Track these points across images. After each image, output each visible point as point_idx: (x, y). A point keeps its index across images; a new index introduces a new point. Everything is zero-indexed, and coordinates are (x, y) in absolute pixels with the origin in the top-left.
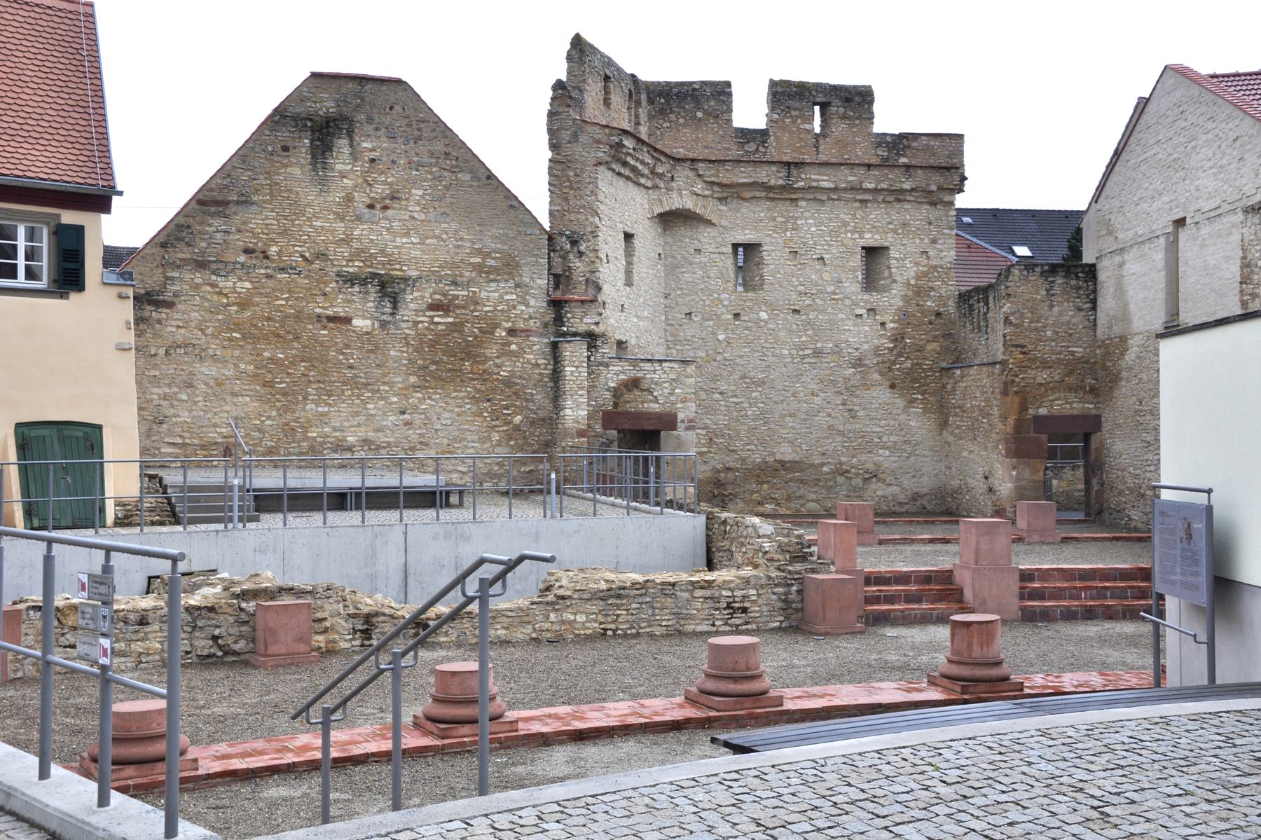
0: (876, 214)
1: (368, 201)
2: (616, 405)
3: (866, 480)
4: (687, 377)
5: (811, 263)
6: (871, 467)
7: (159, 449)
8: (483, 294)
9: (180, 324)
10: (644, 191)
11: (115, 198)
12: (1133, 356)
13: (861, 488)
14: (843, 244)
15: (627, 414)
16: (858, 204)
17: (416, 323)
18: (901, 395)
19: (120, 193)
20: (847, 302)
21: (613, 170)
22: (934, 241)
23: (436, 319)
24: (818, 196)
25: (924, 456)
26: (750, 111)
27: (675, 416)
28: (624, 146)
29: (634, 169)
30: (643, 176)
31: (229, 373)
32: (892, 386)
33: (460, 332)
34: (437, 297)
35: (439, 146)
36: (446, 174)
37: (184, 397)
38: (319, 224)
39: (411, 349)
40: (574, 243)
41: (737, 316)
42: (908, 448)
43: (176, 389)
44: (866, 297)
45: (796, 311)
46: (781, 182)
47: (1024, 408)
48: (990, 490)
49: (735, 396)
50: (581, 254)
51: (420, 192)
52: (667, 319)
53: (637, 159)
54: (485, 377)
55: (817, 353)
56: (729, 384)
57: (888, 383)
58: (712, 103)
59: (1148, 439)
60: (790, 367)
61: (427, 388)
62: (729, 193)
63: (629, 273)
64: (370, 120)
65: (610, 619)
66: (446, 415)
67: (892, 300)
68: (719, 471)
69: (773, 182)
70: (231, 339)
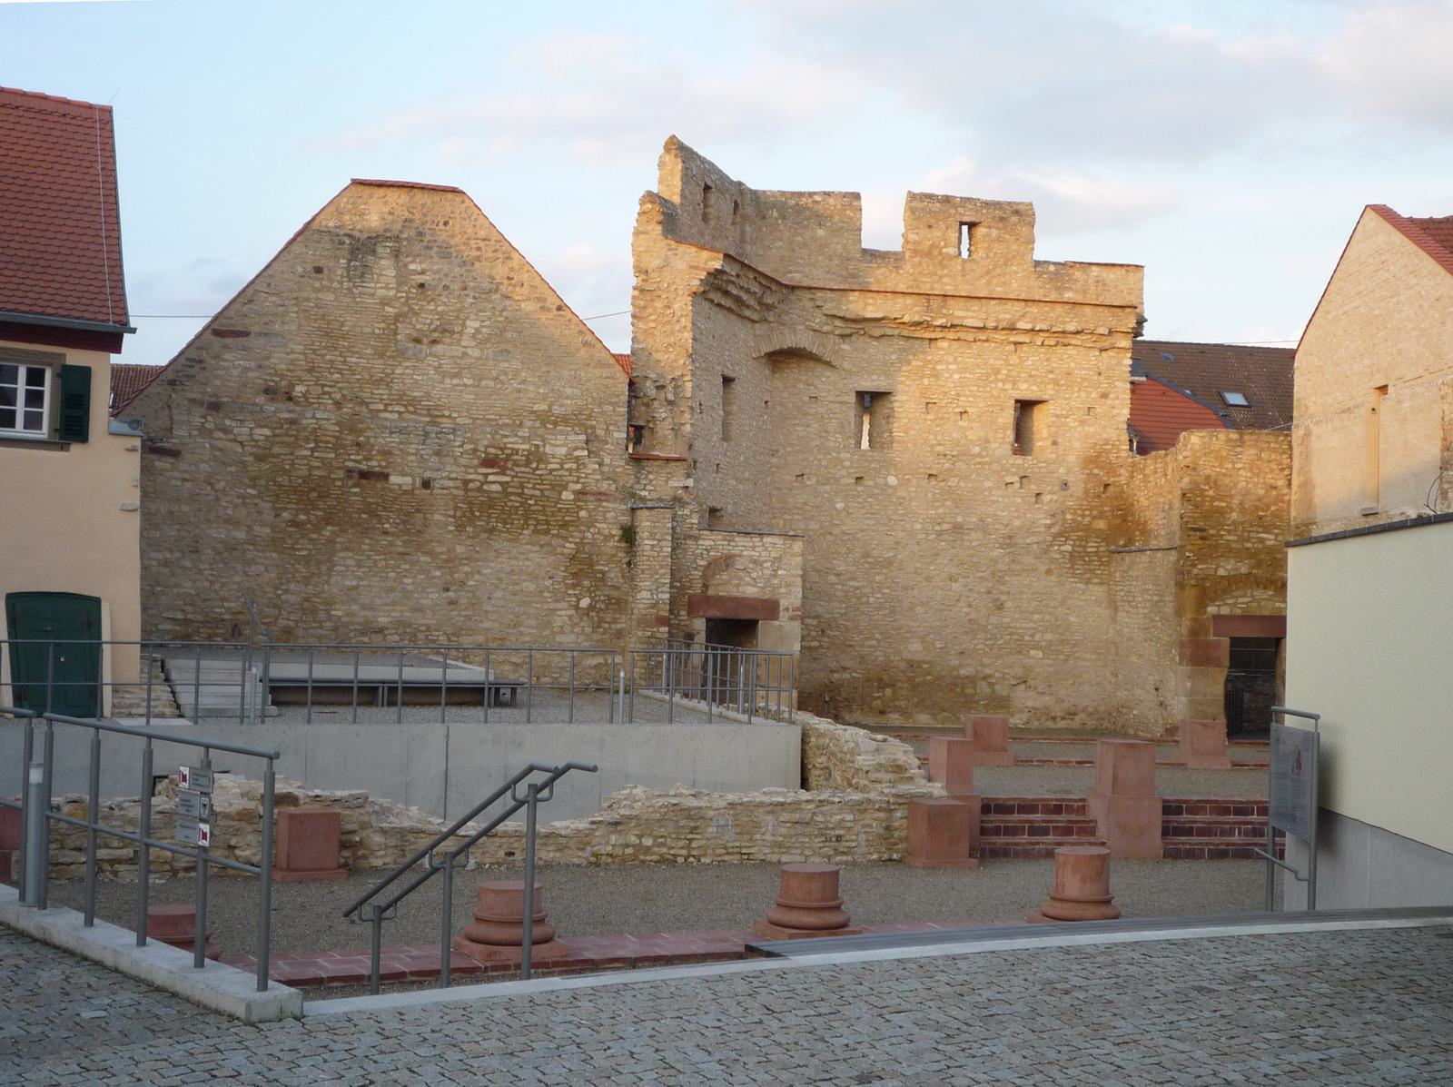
0: (1033, 358)
1: (415, 335)
2: (706, 586)
6: (1019, 672)
7: (156, 625)
8: (548, 449)
9: (187, 476)
10: (749, 325)
11: (126, 336)
14: (992, 396)
17: (466, 482)
19: (133, 331)
21: (712, 301)
22: (1104, 396)
23: (491, 478)
24: (962, 335)
25: (1085, 659)
29: (738, 300)
30: (748, 307)
31: (240, 535)
37: (187, 564)
38: (354, 360)
39: (459, 513)
43: (178, 555)
44: (1019, 460)
47: (1201, 605)
49: (853, 579)
55: (957, 528)
63: (726, 426)
65: (681, 843)
68: (832, 671)
70: (243, 497)
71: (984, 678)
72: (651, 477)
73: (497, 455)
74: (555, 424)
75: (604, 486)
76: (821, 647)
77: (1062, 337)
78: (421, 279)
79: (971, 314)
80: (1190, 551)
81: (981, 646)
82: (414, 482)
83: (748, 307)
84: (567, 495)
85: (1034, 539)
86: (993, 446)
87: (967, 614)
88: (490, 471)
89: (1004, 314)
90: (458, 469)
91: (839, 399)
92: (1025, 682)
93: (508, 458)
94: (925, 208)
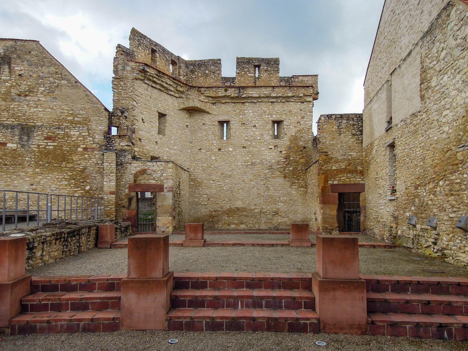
0: (278, 107)
1: (18, 92)
2: (135, 181)
4: (168, 168)
5: (250, 127)
6: (274, 210)
10: (175, 98)
13: (271, 219)
14: (264, 120)
16: (270, 104)
17: (39, 146)
18: (288, 181)
20: (266, 143)
23: (49, 144)
24: (253, 101)
26: (229, 70)
27: (163, 186)
29: (163, 86)
32: (285, 177)
34: (50, 134)
35: (52, 69)
36: (56, 81)
40: (122, 113)
41: (220, 149)
42: (292, 202)
44: (274, 141)
46: (236, 95)
47: (326, 181)
49: (219, 182)
50: (126, 117)
51: (43, 89)
53: (162, 81)
54: (72, 169)
55: (253, 164)
56: (216, 177)
58: (212, 67)
61: (44, 174)
62: (216, 100)
64: (19, 57)
66: (54, 186)
67: (285, 142)
69: (233, 95)
71: (263, 213)
72: (113, 142)
75: (94, 146)
76: (208, 204)
77: (287, 99)
78: (20, 73)
80: (321, 161)
82: (17, 146)
83: (171, 91)
84: (80, 149)
85: (280, 166)
86: (265, 136)
88: (49, 141)
89: (266, 92)
90: (36, 141)
93: (56, 136)
94: (242, 63)
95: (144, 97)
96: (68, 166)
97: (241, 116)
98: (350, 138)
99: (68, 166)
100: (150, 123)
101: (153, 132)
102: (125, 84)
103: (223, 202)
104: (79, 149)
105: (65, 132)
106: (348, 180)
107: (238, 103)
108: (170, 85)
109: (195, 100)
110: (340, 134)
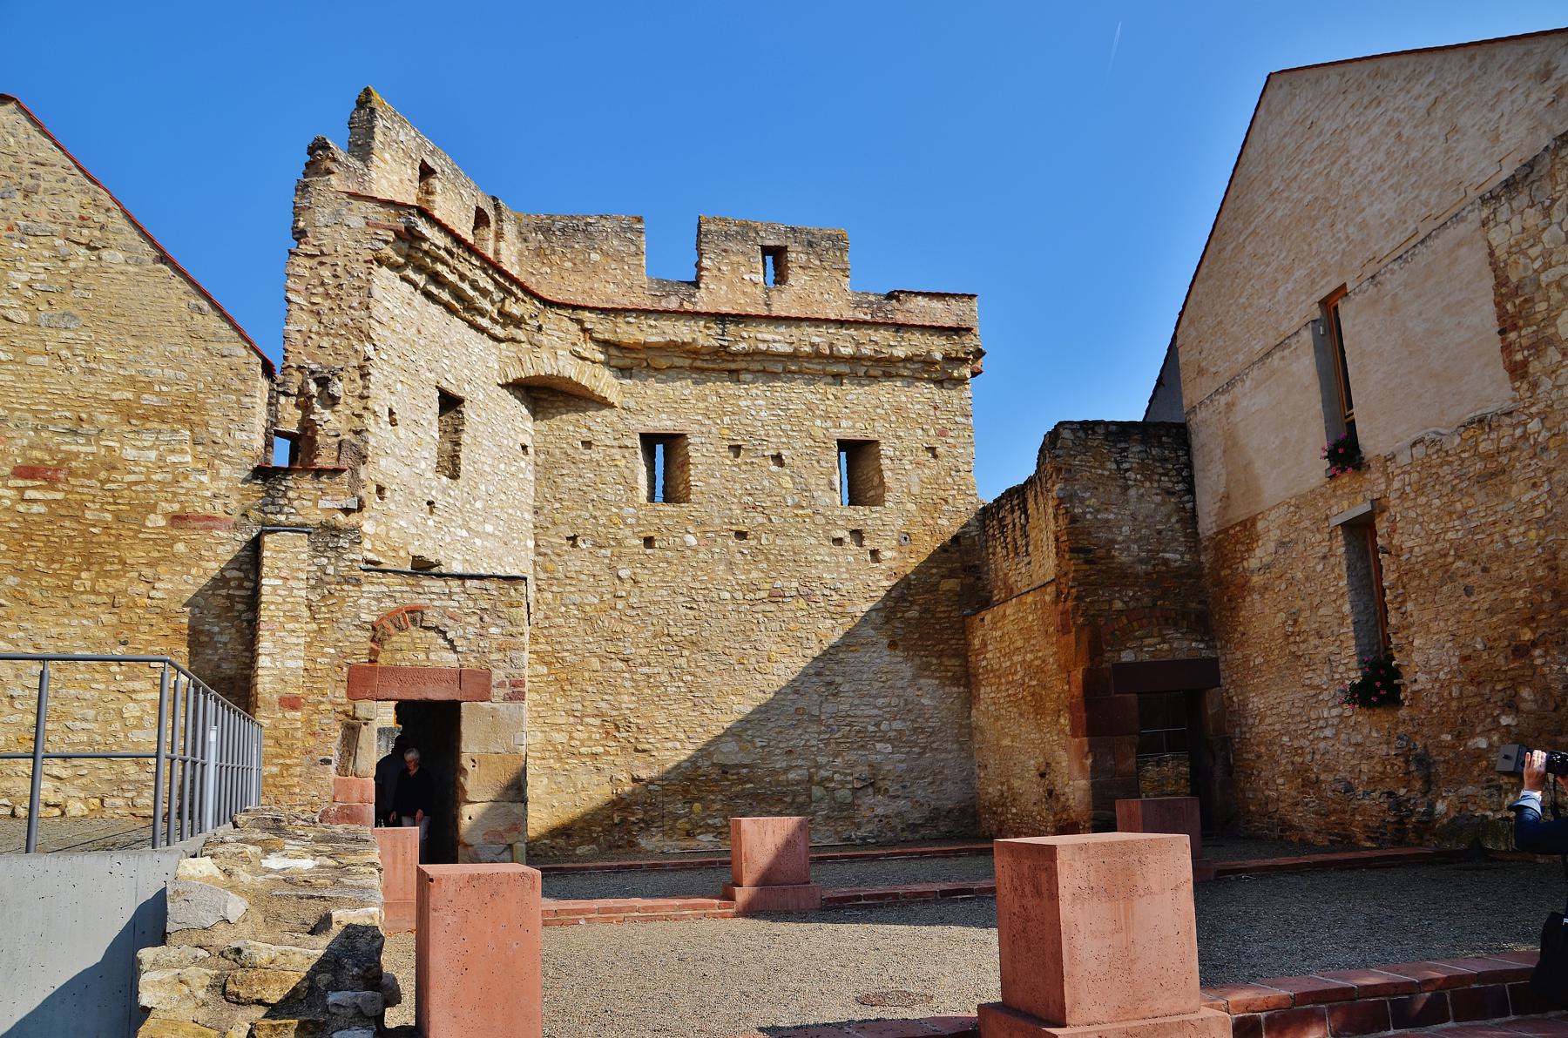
3: (855, 790)
5: (763, 462)
6: (862, 770)
12: (1271, 546)
13: (852, 804)
15: (394, 671)
16: (830, 380)
18: (906, 659)
22: (942, 433)
23: (29, 494)
25: (945, 750)
27: (488, 675)
28: (425, 239)
29: (458, 295)
33: (76, 518)
41: (649, 542)
42: (922, 739)
44: (850, 512)
45: (741, 535)
47: (1095, 648)
48: (1050, 793)
52: (537, 545)
55: (776, 597)
57: (886, 641)
59: (1317, 681)
60: (733, 617)
71: (820, 783)
73: (42, 461)
74: (145, 418)
76: (607, 753)
79: (777, 338)
81: (813, 742)
84: (157, 521)
87: (794, 702)
88: (29, 483)
89: (818, 338)
91: (621, 443)
92: (872, 784)
95: (399, 328)
96: (101, 585)
97: (727, 420)
98: (1158, 505)
99: (101, 585)
100: (413, 425)
101: (423, 465)
102: (336, 276)
103: (670, 745)
104: (152, 516)
105: (99, 446)
106: (1166, 646)
107: (713, 370)
108: (484, 293)
109: (559, 354)
110: (1126, 488)
